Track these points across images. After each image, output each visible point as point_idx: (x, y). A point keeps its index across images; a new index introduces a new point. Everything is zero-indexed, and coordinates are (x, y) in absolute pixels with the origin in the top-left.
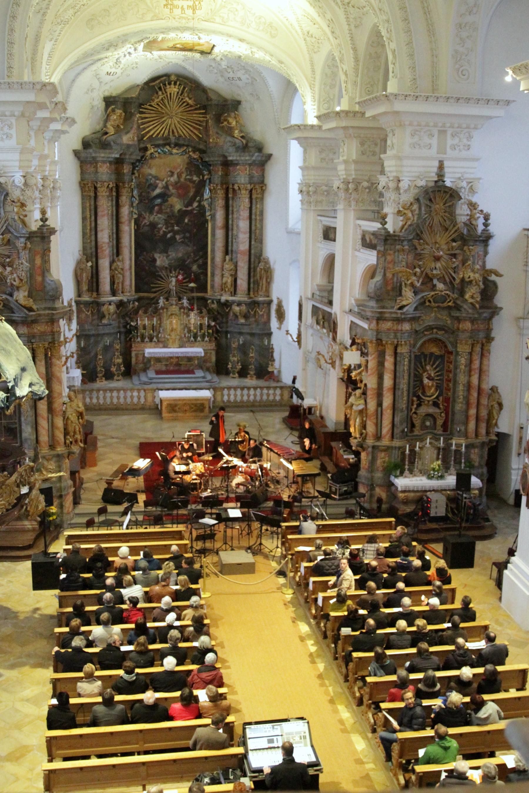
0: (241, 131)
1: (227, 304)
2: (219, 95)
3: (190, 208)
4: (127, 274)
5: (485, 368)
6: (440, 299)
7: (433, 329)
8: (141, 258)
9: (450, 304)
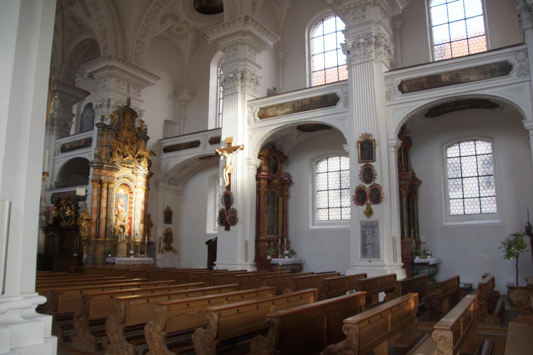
9: (133, 166)
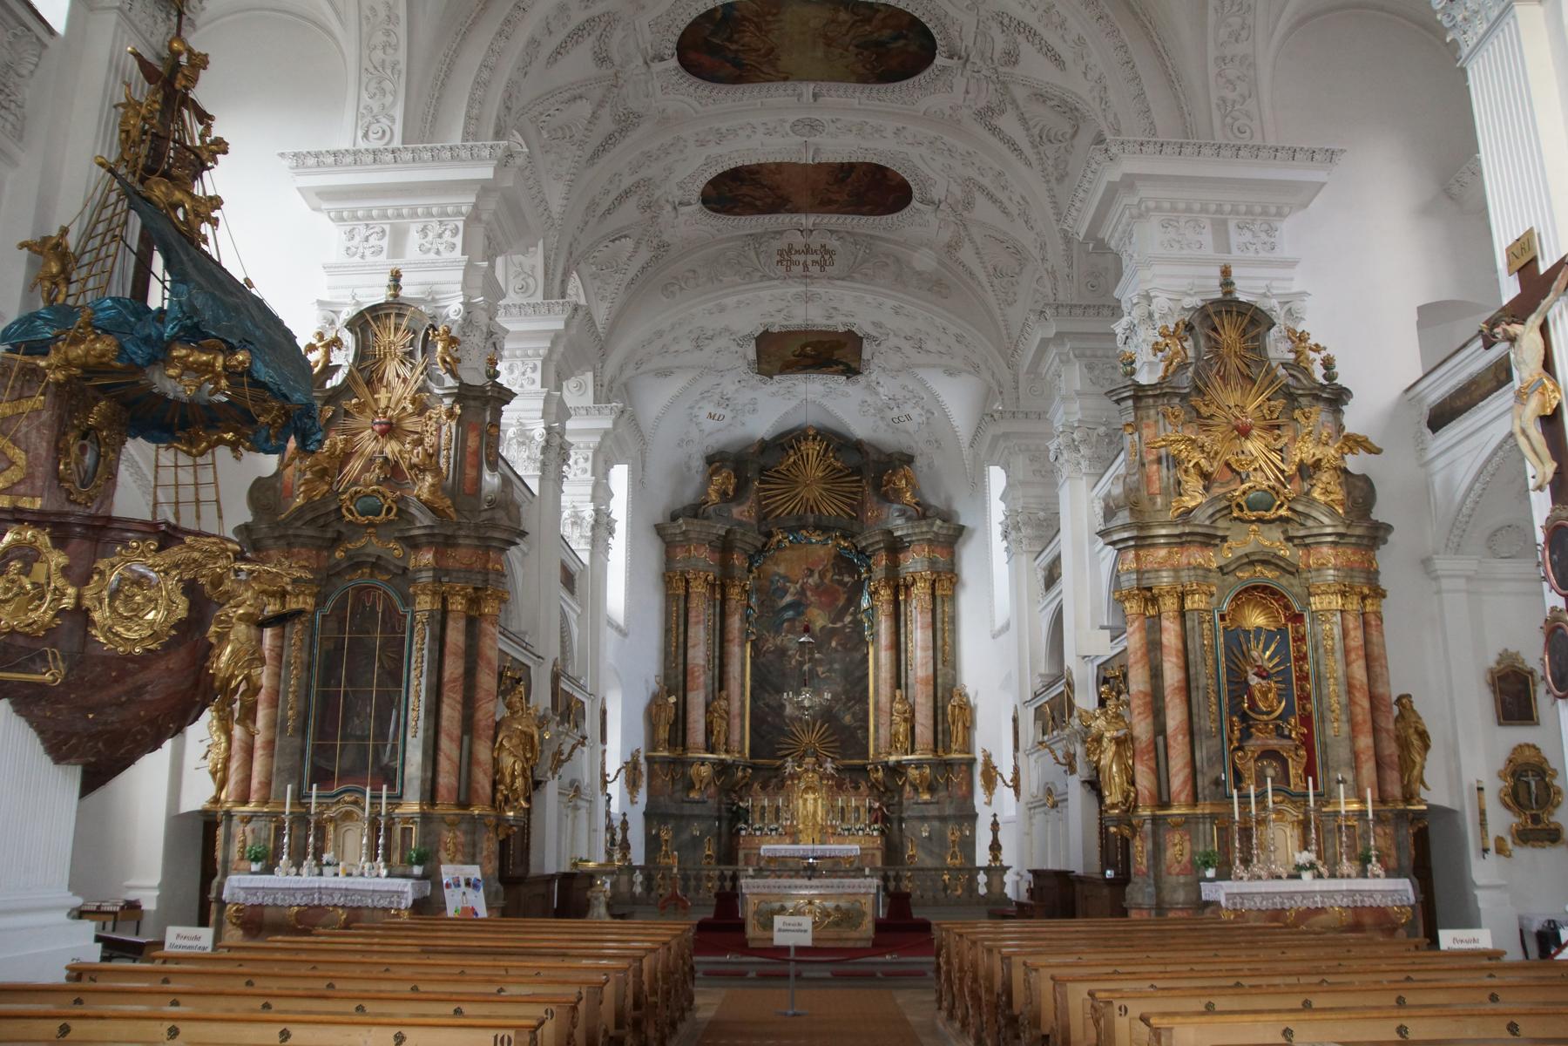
0: (914, 495)
1: (897, 770)
2: (879, 451)
3: (839, 625)
4: (736, 722)
5: (1376, 651)
6: (1259, 508)
7: (1252, 563)
8: (761, 703)
9: (1283, 512)
